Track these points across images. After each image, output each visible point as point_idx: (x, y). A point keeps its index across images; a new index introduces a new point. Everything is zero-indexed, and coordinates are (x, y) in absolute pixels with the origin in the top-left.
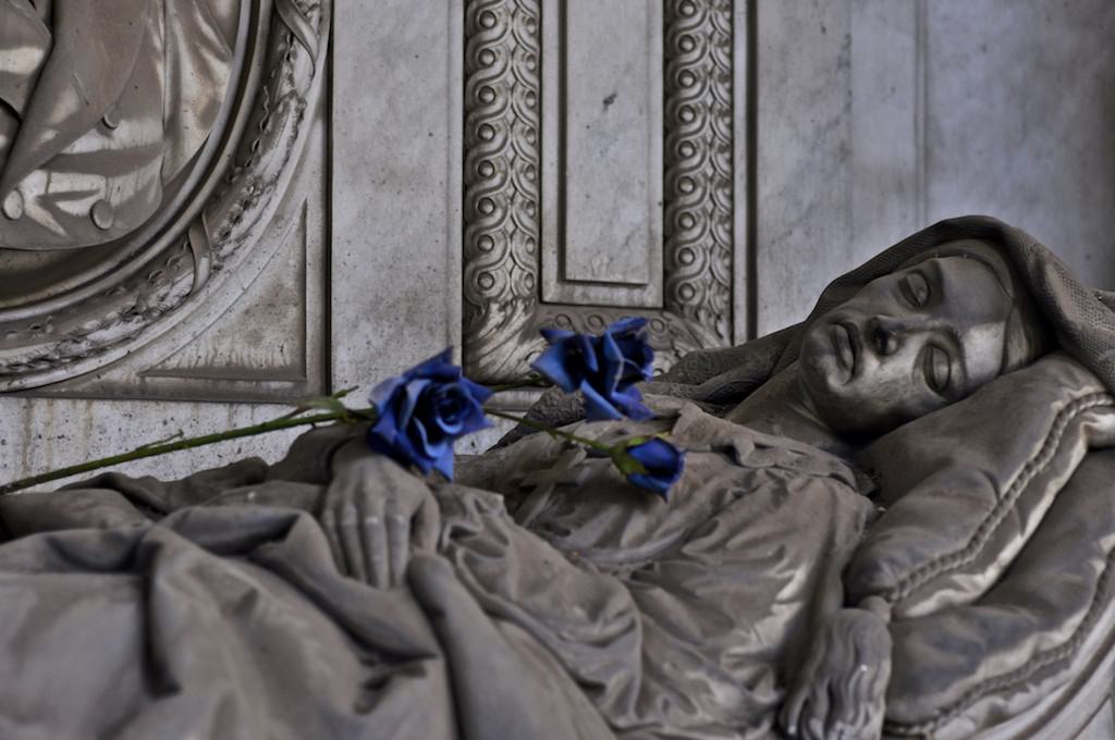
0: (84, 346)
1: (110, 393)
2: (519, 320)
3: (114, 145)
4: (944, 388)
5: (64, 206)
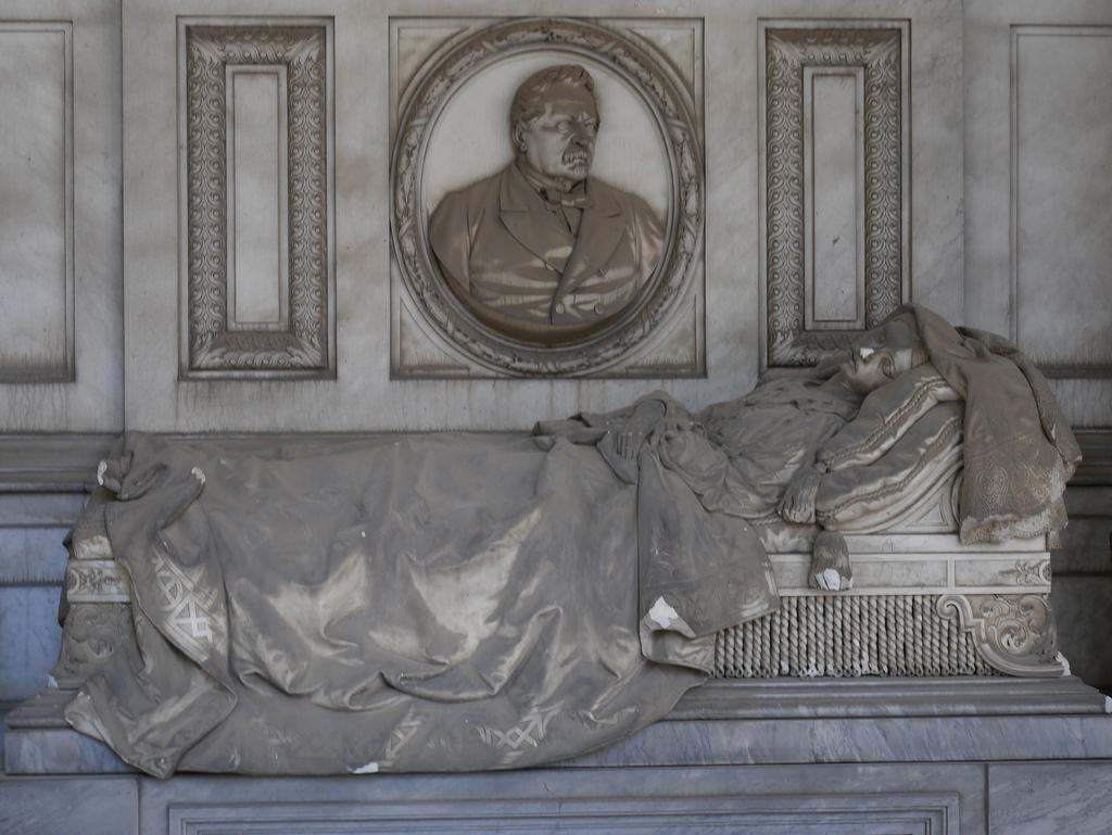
0: (599, 359)
1: (613, 377)
2: (791, 339)
4: (889, 375)
5: (582, 307)
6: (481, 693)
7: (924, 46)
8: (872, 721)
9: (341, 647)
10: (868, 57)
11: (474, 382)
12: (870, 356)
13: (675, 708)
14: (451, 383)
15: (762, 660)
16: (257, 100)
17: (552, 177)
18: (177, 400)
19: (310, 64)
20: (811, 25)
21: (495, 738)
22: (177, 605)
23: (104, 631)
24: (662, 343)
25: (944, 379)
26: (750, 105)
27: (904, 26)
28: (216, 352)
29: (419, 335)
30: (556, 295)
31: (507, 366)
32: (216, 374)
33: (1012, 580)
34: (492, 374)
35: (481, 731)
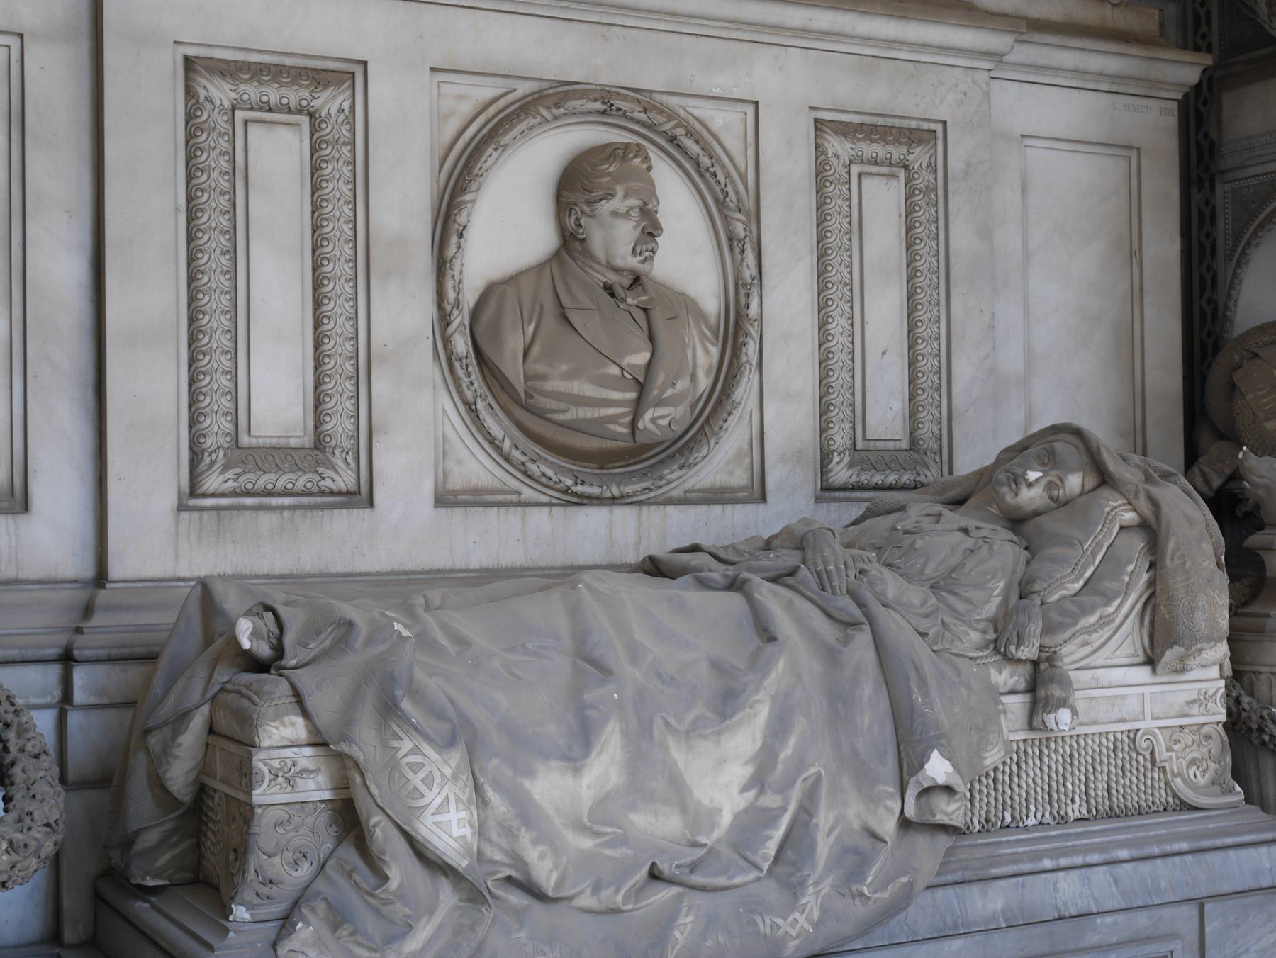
2: (847, 459)
3: (676, 392)
5: (660, 422)
6: (753, 875)
7: (960, 150)
8: (1105, 868)
9: (605, 834)
10: (911, 157)
11: (528, 509)
12: (1037, 480)
13: (939, 874)
14: (503, 510)
15: (988, 811)
16: (277, 155)
17: (617, 270)
18: (177, 534)
19: (342, 117)
20: (856, 119)
21: (775, 927)
22: (433, 798)
23: (300, 839)
24: (719, 464)
25: (1130, 504)
26: (805, 201)
27: (939, 128)
28: (229, 474)
29: (464, 453)
30: (638, 407)
31: (566, 491)
32: (224, 501)
33: (1195, 710)
34: (545, 499)
35: (759, 920)
